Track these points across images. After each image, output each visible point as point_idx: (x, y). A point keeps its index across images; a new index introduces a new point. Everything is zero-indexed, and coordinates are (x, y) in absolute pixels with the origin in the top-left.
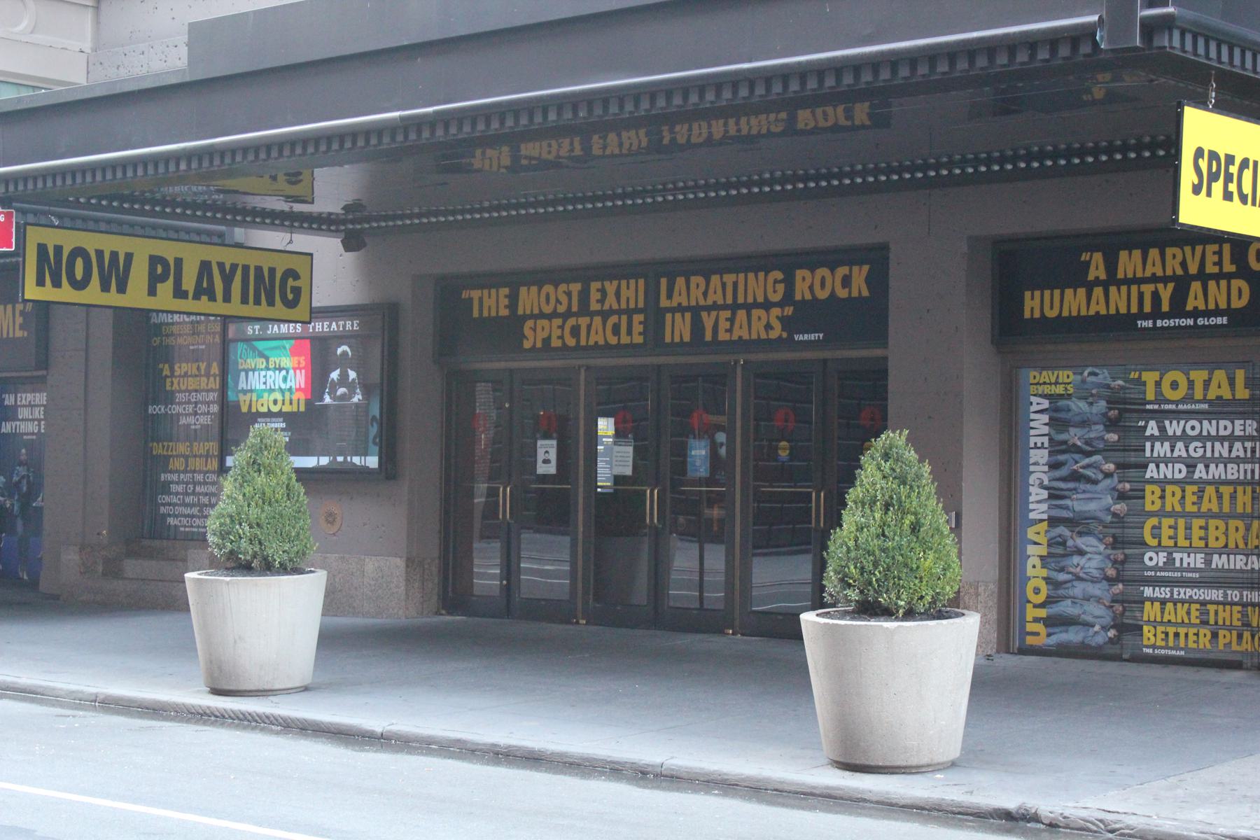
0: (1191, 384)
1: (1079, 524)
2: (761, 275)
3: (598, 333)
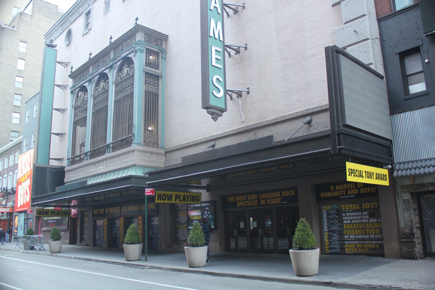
0: (350, 207)
1: (333, 231)
3: (249, 204)
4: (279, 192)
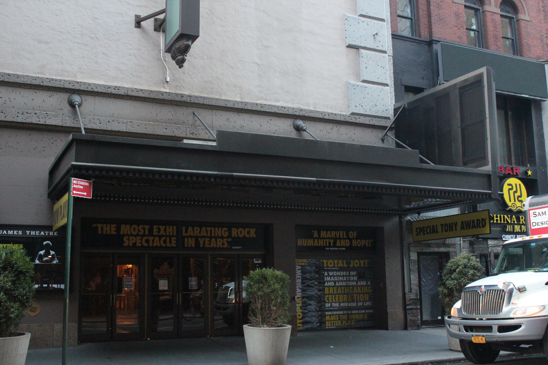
0: (334, 263)
1: (310, 298)
2: (220, 228)
3: (157, 242)
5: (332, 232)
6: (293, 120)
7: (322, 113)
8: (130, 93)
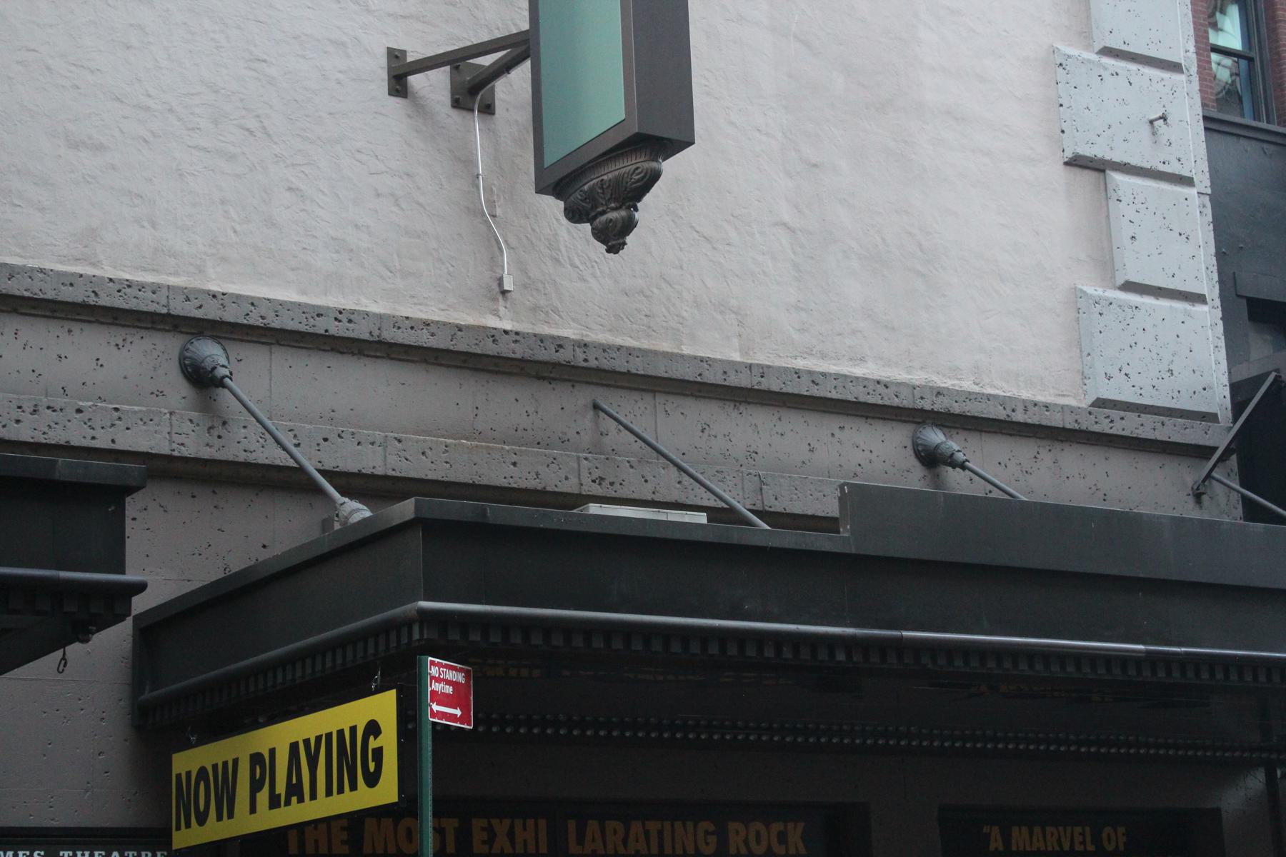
4: (706, 825)
5: (1049, 829)
6: (911, 427)
7: (1003, 401)
8: (390, 335)
